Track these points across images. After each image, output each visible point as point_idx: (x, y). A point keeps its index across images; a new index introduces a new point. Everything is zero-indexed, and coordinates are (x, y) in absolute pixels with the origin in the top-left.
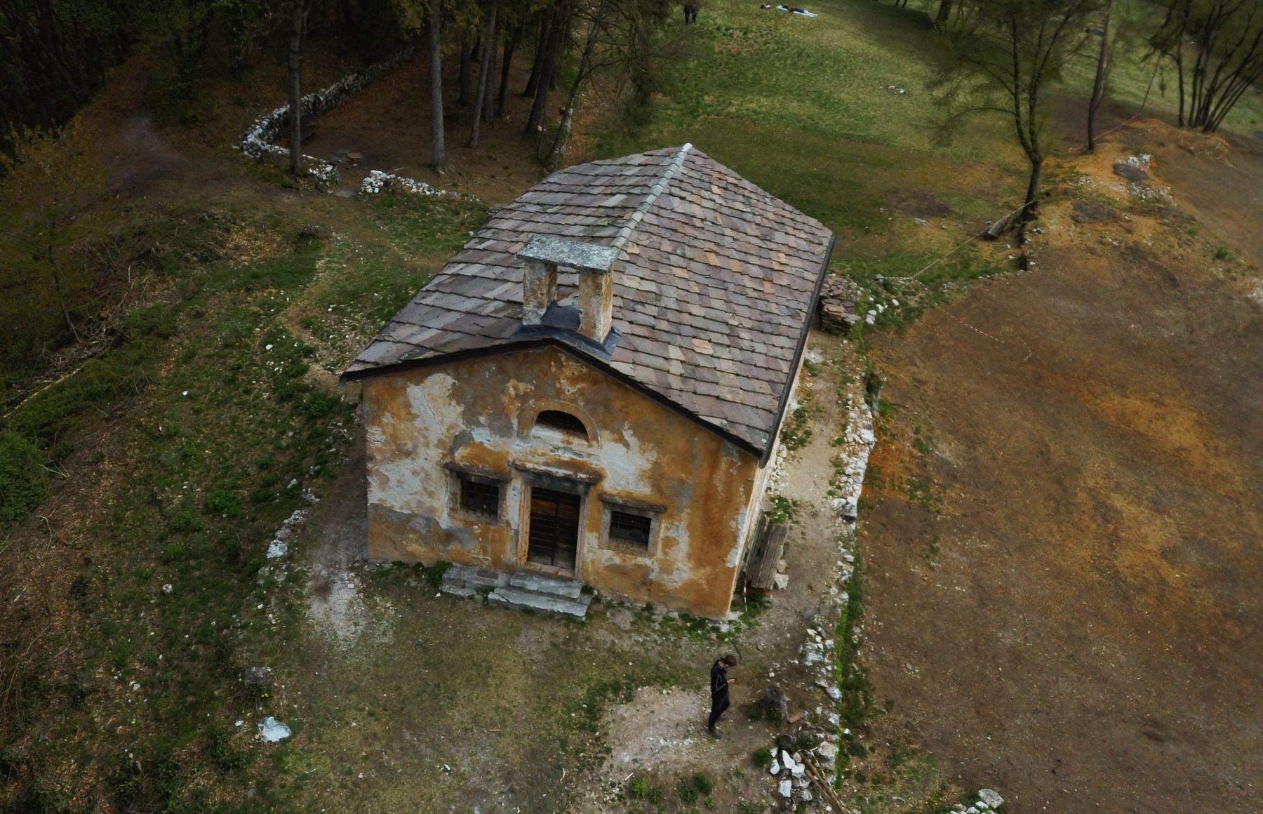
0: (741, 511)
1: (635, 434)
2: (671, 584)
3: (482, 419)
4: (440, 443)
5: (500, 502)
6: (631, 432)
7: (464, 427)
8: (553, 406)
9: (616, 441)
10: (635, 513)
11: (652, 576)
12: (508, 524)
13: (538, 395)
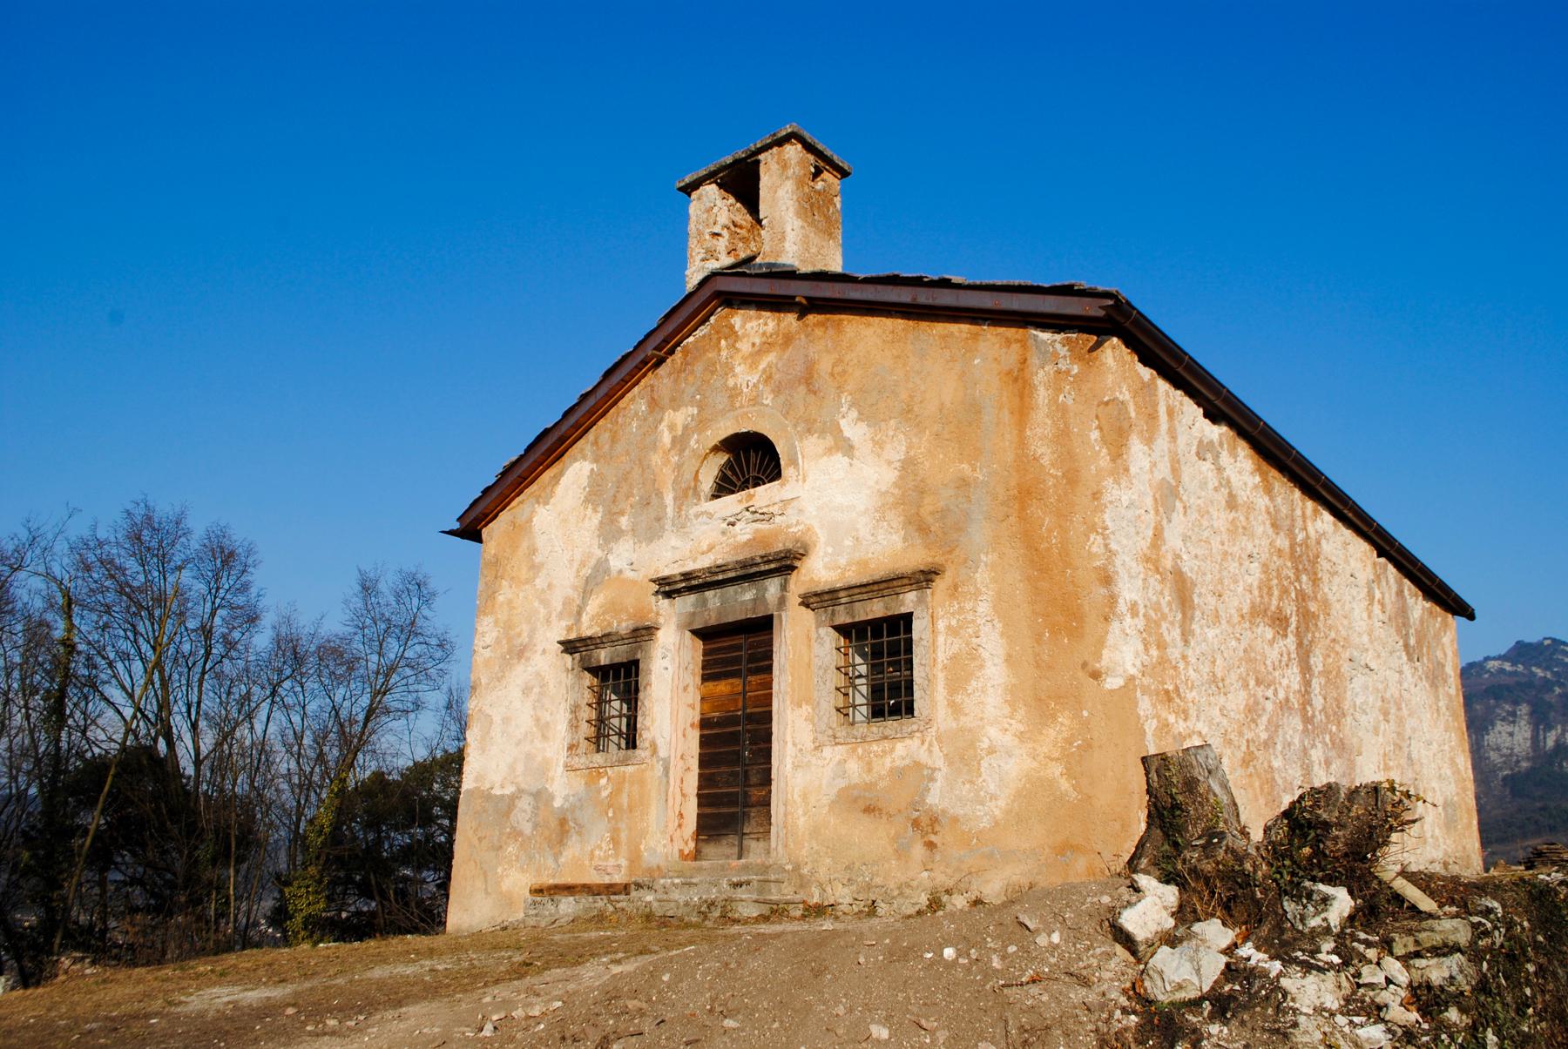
0: (1107, 498)
1: (861, 418)
2: (980, 811)
3: (624, 522)
4: (567, 602)
5: (641, 695)
6: (854, 414)
7: (599, 553)
8: (727, 428)
9: (829, 451)
10: (876, 609)
11: (935, 798)
12: (654, 748)
13: (701, 423)
